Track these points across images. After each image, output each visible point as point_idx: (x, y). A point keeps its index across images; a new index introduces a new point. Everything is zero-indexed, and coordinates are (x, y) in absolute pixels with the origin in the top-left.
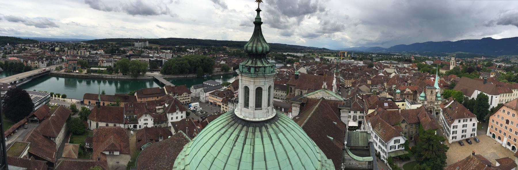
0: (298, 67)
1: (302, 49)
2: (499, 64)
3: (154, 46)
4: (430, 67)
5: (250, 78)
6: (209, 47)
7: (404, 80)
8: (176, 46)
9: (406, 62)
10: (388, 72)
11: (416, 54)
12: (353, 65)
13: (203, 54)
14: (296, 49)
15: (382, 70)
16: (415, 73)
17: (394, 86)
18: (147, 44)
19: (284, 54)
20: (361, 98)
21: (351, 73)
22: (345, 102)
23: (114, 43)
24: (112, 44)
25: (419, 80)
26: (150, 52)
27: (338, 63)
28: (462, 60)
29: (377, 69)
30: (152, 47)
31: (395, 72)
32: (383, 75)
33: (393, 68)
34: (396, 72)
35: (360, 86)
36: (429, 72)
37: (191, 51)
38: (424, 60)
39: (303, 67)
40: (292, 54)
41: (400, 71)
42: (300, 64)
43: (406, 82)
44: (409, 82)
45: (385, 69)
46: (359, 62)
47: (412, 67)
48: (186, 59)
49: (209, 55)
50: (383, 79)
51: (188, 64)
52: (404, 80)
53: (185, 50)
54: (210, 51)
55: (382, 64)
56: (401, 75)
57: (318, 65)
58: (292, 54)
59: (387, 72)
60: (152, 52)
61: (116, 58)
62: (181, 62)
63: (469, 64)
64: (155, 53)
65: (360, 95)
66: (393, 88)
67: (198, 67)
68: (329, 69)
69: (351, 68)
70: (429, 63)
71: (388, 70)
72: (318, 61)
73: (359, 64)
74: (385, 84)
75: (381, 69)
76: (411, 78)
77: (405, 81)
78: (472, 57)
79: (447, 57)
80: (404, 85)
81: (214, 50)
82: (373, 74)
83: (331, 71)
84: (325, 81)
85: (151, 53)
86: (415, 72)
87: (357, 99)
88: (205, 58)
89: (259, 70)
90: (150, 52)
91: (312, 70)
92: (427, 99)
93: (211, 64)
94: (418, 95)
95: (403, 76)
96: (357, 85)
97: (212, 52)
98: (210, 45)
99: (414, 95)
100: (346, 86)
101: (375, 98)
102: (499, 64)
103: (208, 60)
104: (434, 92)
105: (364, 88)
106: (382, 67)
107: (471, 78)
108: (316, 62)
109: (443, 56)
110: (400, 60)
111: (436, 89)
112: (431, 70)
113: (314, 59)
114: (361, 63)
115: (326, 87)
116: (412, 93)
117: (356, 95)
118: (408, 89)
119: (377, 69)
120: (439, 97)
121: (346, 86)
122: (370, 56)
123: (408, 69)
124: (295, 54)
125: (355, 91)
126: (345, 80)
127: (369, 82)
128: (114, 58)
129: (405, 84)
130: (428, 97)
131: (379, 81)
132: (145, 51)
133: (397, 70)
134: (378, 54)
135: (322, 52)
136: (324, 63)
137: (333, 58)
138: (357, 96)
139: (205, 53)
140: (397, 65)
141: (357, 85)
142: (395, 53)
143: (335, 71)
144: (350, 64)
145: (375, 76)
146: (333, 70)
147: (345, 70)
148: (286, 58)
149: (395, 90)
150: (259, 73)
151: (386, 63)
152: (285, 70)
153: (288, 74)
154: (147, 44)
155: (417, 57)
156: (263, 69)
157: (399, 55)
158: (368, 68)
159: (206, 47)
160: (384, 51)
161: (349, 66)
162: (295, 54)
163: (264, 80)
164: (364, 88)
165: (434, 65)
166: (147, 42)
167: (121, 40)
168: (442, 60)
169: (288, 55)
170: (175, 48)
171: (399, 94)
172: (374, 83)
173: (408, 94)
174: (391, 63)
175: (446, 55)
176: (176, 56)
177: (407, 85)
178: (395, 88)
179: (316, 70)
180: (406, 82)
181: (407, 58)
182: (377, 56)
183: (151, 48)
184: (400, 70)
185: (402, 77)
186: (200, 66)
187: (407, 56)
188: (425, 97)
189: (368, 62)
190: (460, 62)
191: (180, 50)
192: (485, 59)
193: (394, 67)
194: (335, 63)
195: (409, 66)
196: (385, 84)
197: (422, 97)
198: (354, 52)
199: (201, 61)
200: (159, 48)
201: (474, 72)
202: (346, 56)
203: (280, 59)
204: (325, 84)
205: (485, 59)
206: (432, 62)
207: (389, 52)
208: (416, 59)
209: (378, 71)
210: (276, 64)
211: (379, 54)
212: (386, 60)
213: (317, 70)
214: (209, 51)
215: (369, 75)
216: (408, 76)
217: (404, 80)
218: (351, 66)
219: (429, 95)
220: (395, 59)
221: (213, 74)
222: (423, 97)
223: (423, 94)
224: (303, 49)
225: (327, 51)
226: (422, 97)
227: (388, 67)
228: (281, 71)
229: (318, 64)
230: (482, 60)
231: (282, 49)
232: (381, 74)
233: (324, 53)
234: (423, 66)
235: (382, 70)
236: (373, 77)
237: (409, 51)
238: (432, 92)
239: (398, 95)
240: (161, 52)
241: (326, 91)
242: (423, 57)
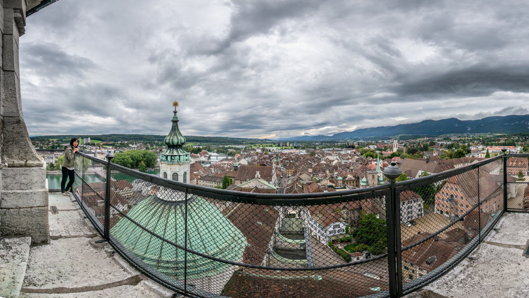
0: (239, 159)
1: (243, 141)
2: (440, 143)
3: (96, 142)
4: (373, 151)
5: (167, 165)
6: (152, 143)
7: (346, 167)
8: (118, 142)
9: (350, 149)
10: (330, 159)
11: (359, 140)
13: (145, 149)
14: (238, 142)
16: (357, 159)
17: (336, 173)
18: (89, 141)
19: (226, 146)
20: (301, 187)
22: (278, 190)
23: (55, 140)
24: (53, 141)
25: (360, 166)
26: (92, 148)
28: (406, 141)
30: (95, 144)
31: (337, 159)
32: (325, 163)
33: (336, 155)
34: (339, 159)
35: (301, 174)
36: (372, 156)
37: (134, 146)
38: (368, 144)
40: (233, 146)
41: (343, 157)
42: (242, 155)
43: (348, 168)
44: (351, 168)
45: (327, 157)
46: (302, 151)
47: (355, 153)
48: (128, 154)
49: (152, 149)
51: (130, 159)
52: (346, 167)
53: (127, 146)
54: (153, 146)
55: (324, 152)
56: (343, 162)
58: (233, 146)
59: (329, 159)
60: (94, 148)
61: (57, 155)
62: (123, 157)
63: (412, 145)
64: (97, 149)
65: (300, 184)
66: (335, 176)
67: (140, 161)
68: (269, 159)
69: (293, 157)
70: (372, 147)
71: (330, 158)
73: (301, 153)
74: (328, 172)
76: (353, 164)
77: (348, 168)
78: (416, 137)
79: (390, 141)
80: (346, 171)
81: (157, 145)
82: (315, 162)
83: (272, 161)
84: (258, 170)
85: (93, 149)
86: (357, 157)
88: (146, 154)
89: (174, 159)
90: (92, 148)
91: (253, 161)
92: (370, 184)
93: (153, 159)
94: (360, 181)
95: (345, 163)
97: (155, 147)
98: (153, 140)
99: (356, 181)
100: (287, 176)
101: (315, 186)
102: (440, 143)
103: (150, 155)
104: (376, 176)
105: (304, 176)
106: (323, 154)
107: (415, 159)
109: (387, 140)
110: (342, 147)
111: (378, 173)
112: (374, 155)
113: (255, 150)
114: (304, 152)
115: (259, 176)
116: (354, 179)
118: (349, 175)
120: (382, 181)
121: (287, 176)
122: (313, 144)
123: (350, 155)
124: (237, 147)
125: (295, 180)
126: (286, 169)
127: (310, 170)
128: (55, 155)
129: (347, 170)
130: (370, 182)
131: (321, 169)
132: (86, 147)
133: (339, 156)
134: (321, 142)
135: (264, 143)
136: (266, 154)
137: (275, 148)
139: (147, 148)
140: (340, 152)
141: (298, 174)
142: (339, 141)
144: (292, 153)
147: (286, 159)
148: (228, 151)
149: (336, 177)
150: (175, 160)
151: (329, 151)
152: (226, 162)
153: (229, 167)
154: (89, 141)
155: (360, 143)
156: (178, 157)
157: (343, 142)
158: (310, 156)
159: (148, 142)
160: (327, 139)
161: (291, 155)
162: (237, 147)
163: (179, 167)
164: (304, 176)
165: (377, 149)
166: (89, 139)
167: (62, 137)
168: (386, 144)
169: (230, 148)
170: (117, 143)
171: (340, 180)
172: (316, 171)
173: (350, 181)
174: (333, 151)
175: (389, 139)
176: (118, 152)
177: (350, 171)
178: (336, 175)
179: (257, 160)
180: (348, 168)
181: (351, 144)
182: (320, 144)
183: (93, 145)
184: (342, 157)
185: (344, 164)
186: (142, 160)
187: (351, 143)
188: (367, 182)
189: (311, 150)
190: (404, 144)
191: (122, 145)
192: (427, 139)
193: (336, 153)
195: (352, 152)
196: (328, 172)
197: (364, 182)
198: (297, 141)
199: (143, 156)
200: (101, 144)
201: (417, 152)
202: (288, 146)
203: (221, 152)
204: (258, 173)
205: (427, 139)
206: (376, 147)
207: (333, 140)
208: (359, 145)
209: (320, 159)
210: (218, 157)
211: (322, 142)
212: (330, 147)
213: (258, 161)
214: (152, 146)
215: (311, 164)
216: (350, 162)
217: (347, 167)
219: (371, 179)
220: (338, 147)
221: (156, 169)
222: (365, 182)
223: (364, 179)
224: (244, 141)
225: (269, 142)
226: (364, 182)
227: (330, 155)
228: (223, 164)
229: (259, 155)
230: (425, 140)
231: (224, 142)
232: (323, 162)
233: (266, 143)
234: (366, 151)
237: (352, 138)
238: (373, 176)
239: (340, 182)
240: (103, 148)
241: (259, 180)
242: (367, 143)
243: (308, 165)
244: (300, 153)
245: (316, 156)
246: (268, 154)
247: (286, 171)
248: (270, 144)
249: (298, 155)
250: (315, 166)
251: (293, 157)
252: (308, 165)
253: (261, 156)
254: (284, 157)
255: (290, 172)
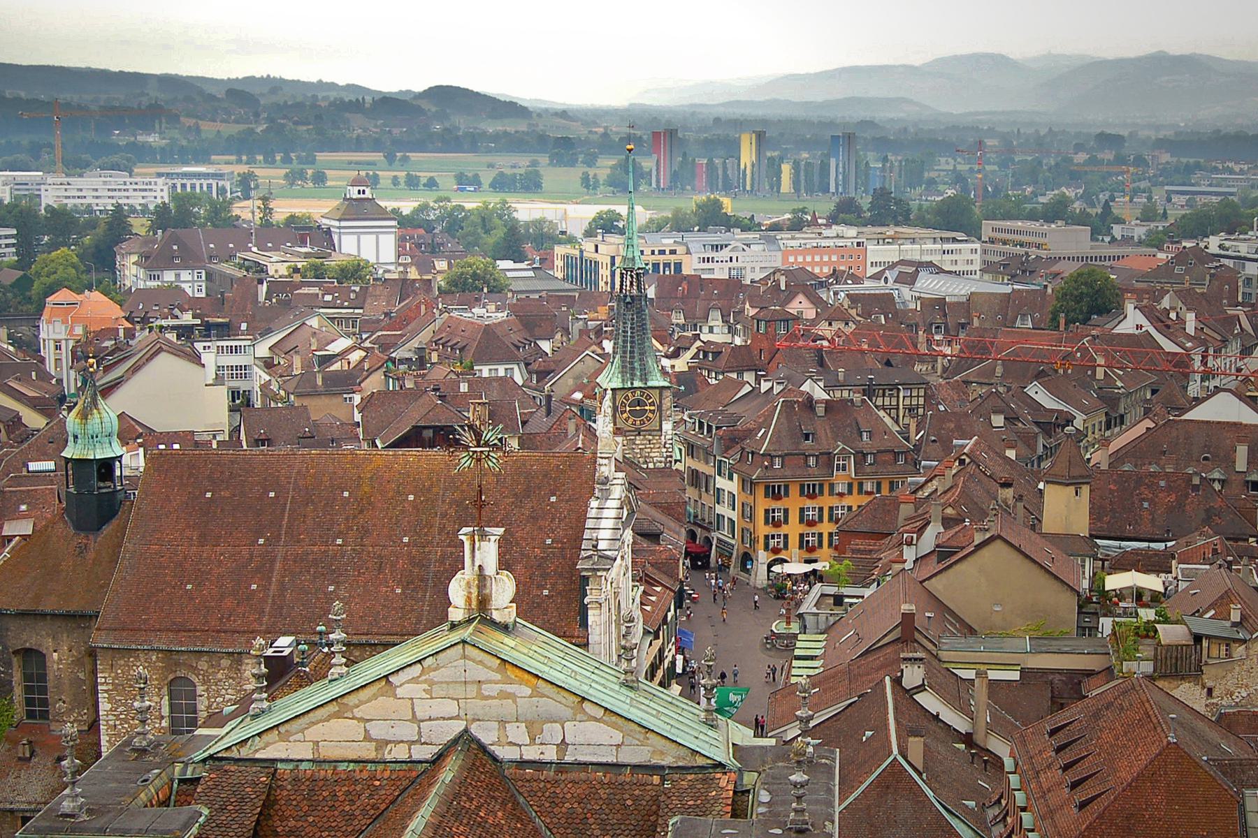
12: (853, 298)
15: (1234, 348)
21: (819, 394)
27: (639, 278)
29: (1168, 346)
39: (177, 352)
50: (1241, 465)
57: (376, 308)
69: (824, 329)
72: (368, 255)
73: (929, 285)
75: (1225, 341)
83: (563, 384)
87: (906, 732)
91: (306, 388)
96: (909, 554)
100: (760, 576)
108: (354, 272)
117: (897, 682)
119: (1168, 346)
121: (760, 576)
126: (748, 484)
138: (906, 695)
143: (610, 379)
144: (803, 283)
145: (1140, 429)
146: (581, 365)
147: (742, 360)
194: (605, 272)
209: (1181, 364)
213: (374, 383)
218: (816, 301)
235: (1234, 348)
236: (1115, 445)
243: (1030, 441)
244: (908, 279)
245: (1132, 321)
246: (497, 288)
247: (748, 513)
248: (518, 163)
249: (885, 302)
250: (1118, 458)
251: (824, 329)
252: (1030, 441)
253: (402, 322)
254: (716, 333)
255: (793, 529)
